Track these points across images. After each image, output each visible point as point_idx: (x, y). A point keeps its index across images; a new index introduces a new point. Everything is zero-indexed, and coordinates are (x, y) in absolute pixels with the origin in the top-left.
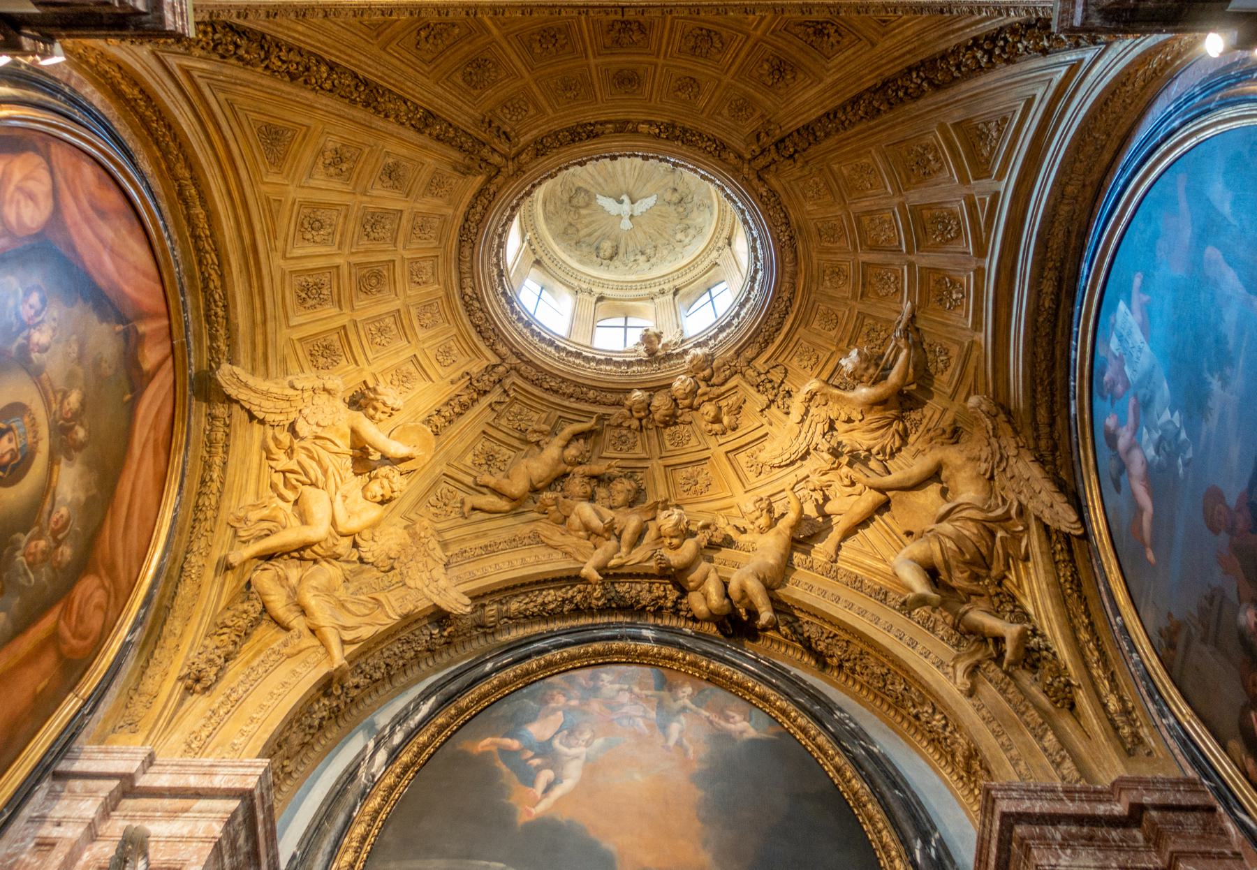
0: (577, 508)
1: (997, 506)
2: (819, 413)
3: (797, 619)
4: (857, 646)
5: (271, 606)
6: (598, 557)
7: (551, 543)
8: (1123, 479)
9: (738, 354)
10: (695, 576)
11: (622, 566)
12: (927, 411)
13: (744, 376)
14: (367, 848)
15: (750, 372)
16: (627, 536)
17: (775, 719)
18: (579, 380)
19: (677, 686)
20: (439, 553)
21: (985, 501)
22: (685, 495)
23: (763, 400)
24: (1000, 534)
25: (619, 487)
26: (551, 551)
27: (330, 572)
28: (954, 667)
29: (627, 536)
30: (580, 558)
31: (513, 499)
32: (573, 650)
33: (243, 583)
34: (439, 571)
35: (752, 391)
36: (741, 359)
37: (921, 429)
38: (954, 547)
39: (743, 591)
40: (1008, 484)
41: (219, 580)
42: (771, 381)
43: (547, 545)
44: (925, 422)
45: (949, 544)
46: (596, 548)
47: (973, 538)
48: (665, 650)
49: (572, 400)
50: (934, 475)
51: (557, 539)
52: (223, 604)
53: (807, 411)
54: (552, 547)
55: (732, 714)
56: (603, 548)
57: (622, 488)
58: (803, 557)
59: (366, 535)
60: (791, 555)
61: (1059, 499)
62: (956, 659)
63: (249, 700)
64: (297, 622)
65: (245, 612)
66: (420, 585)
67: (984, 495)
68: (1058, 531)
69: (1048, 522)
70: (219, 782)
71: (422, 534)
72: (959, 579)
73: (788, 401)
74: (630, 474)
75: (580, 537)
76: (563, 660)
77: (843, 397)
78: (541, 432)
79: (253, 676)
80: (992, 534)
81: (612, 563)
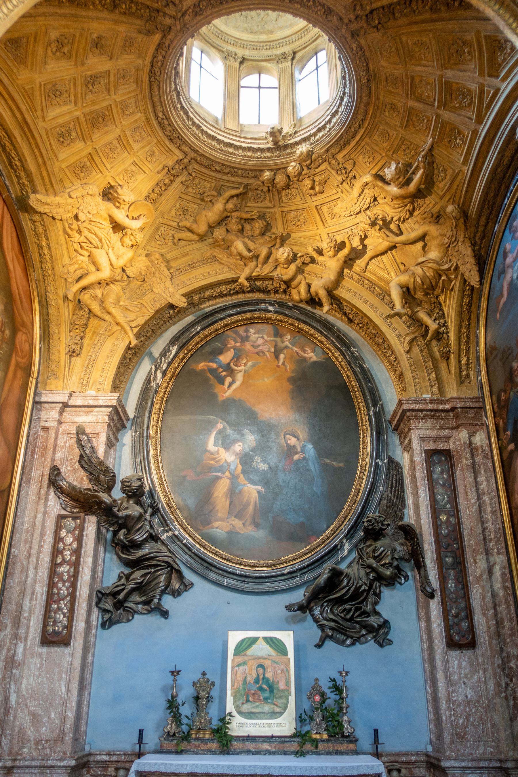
0: (235, 244)
1: (447, 262)
2: (369, 193)
3: (342, 303)
4: (366, 321)
5: (93, 311)
6: (247, 272)
7: (222, 262)
8: (502, 276)
9: (327, 150)
10: (295, 283)
11: (259, 275)
12: (427, 200)
13: (330, 163)
14: (162, 412)
15: (333, 162)
16: (261, 259)
17: (325, 352)
18: (232, 165)
19: (284, 335)
20: (166, 272)
21: (442, 258)
22: (292, 227)
23: (340, 178)
24: (443, 278)
25: (257, 225)
26: (222, 266)
27: (115, 288)
28: (404, 339)
29: (261, 259)
30: (238, 272)
31: (198, 235)
32: (236, 318)
33: (77, 301)
34: (168, 283)
35: (334, 173)
36: (329, 153)
37: (422, 209)
38: (420, 282)
39: (317, 294)
40: (454, 253)
41: (66, 304)
42: (345, 168)
43: (221, 263)
44: (425, 206)
45: (419, 280)
46: (245, 265)
47: (430, 277)
48: (279, 317)
49: (229, 175)
50: (422, 238)
51: (225, 260)
52: (71, 314)
53: (363, 191)
54: (223, 264)
55: (307, 349)
56: (249, 266)
57: (259, 225)
58: (349, 272)
59: (128, 265)
60: (343, 270)
61: (475, 268)
62: (407, 335)
63: (99, 359)
64: (107, 317)
65: (82, 316)
66: (160, 292)
67: (442, 255)
68: (469, 284)
69: (466, 278)
70: (101, 403)
71: (156, 262)
72: (419, 295)
73: (353, 181)
74: (262, 217)
75: (237, 259)
76: (232, 323)
77: (383, 188)
78: (213, 196)
79: (97, 348)
80: (440, 276)
81: (254, 274)
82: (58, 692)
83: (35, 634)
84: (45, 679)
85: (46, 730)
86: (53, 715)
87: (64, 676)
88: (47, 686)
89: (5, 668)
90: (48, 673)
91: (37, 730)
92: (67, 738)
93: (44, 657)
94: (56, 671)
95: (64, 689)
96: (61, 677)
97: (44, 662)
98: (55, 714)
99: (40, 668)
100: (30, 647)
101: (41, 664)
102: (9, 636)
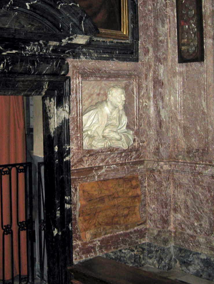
82: (200, 107)
83: (173, 55)
84: (188, 96)
85: (195, 141)
86: (199, 128)
87: (203, 92)
88: (190, 102)
89: (154, 87)
90: (189, 90)
91: (188, 141)
92: (211, 149)
93: (185, 75)
94: (196, 87)
95: (204, 104)
96: (201, 93)
97: (185, 80)
98: (200, 127)
99: (183, 85)
100: (172, 67)
101: (184, 82)
102: (153, 59)
